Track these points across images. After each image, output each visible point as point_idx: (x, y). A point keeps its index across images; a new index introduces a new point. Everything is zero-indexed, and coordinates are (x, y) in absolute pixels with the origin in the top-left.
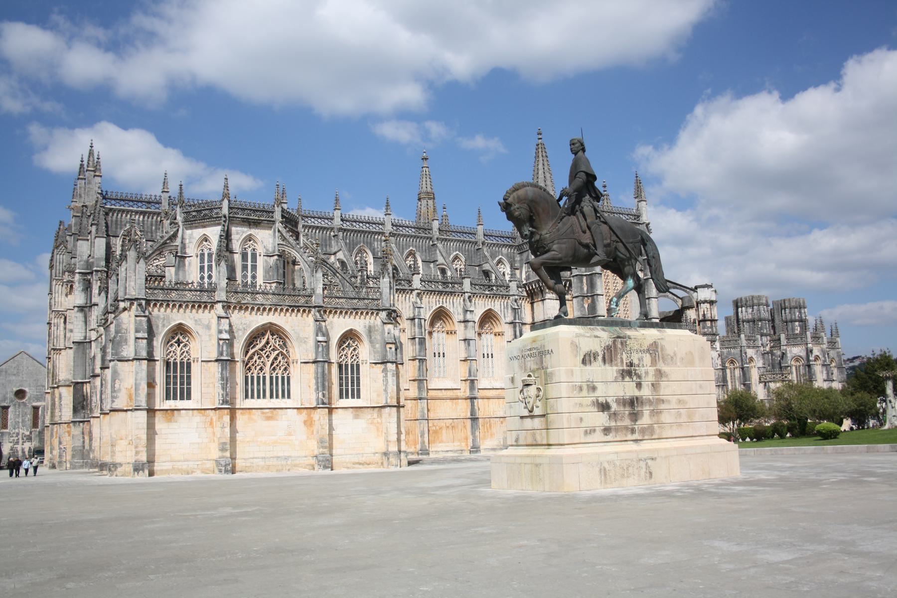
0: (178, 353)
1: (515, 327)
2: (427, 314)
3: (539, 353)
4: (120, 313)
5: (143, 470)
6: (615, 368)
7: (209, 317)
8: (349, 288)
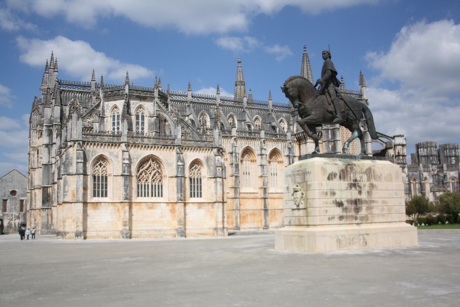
1: (289, 158)
2: (240, 151)
3: (303, 173)
4: (68, 148)
5: (81, 236)
6: (346, 182)
7: (117, 151)
8: (196, 136)
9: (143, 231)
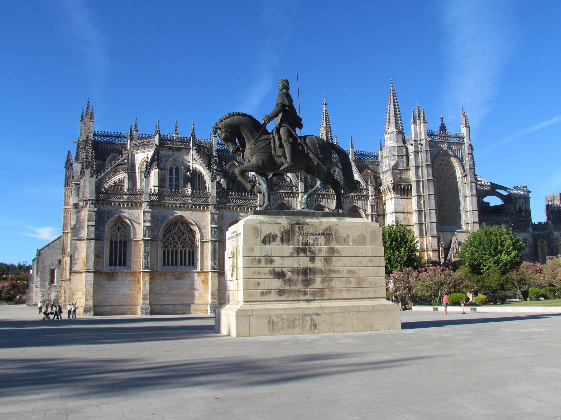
0: (119, 235)
5: (90, 311)
6: (291, 246)
9: (168, 306)
